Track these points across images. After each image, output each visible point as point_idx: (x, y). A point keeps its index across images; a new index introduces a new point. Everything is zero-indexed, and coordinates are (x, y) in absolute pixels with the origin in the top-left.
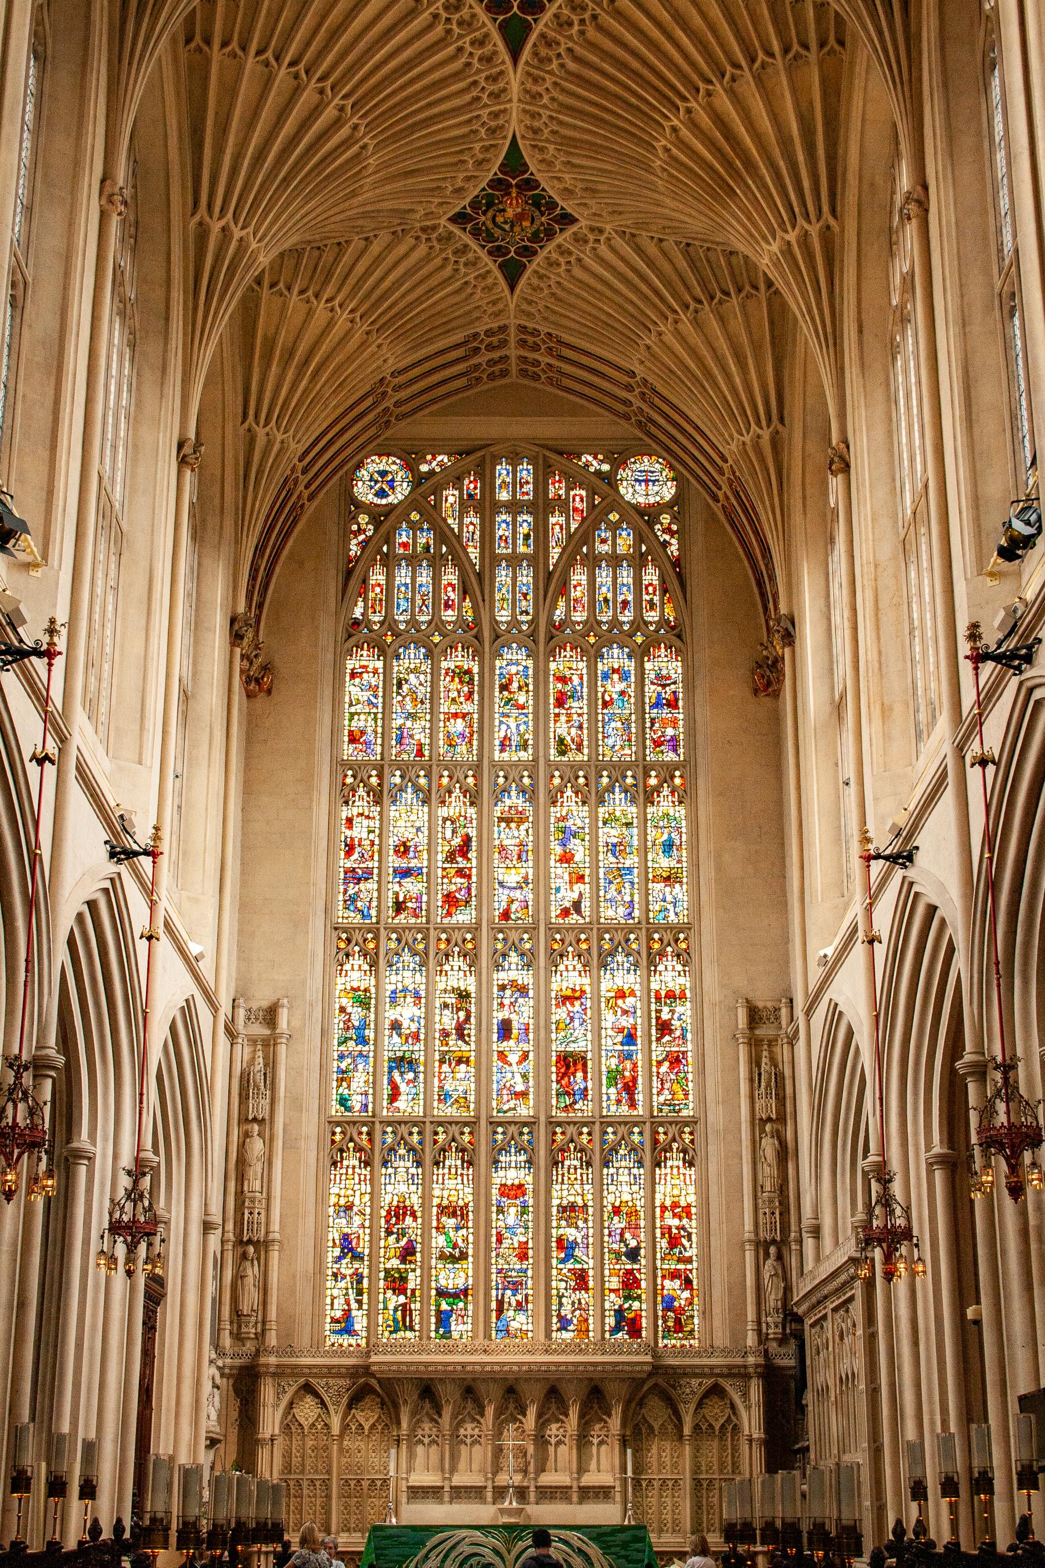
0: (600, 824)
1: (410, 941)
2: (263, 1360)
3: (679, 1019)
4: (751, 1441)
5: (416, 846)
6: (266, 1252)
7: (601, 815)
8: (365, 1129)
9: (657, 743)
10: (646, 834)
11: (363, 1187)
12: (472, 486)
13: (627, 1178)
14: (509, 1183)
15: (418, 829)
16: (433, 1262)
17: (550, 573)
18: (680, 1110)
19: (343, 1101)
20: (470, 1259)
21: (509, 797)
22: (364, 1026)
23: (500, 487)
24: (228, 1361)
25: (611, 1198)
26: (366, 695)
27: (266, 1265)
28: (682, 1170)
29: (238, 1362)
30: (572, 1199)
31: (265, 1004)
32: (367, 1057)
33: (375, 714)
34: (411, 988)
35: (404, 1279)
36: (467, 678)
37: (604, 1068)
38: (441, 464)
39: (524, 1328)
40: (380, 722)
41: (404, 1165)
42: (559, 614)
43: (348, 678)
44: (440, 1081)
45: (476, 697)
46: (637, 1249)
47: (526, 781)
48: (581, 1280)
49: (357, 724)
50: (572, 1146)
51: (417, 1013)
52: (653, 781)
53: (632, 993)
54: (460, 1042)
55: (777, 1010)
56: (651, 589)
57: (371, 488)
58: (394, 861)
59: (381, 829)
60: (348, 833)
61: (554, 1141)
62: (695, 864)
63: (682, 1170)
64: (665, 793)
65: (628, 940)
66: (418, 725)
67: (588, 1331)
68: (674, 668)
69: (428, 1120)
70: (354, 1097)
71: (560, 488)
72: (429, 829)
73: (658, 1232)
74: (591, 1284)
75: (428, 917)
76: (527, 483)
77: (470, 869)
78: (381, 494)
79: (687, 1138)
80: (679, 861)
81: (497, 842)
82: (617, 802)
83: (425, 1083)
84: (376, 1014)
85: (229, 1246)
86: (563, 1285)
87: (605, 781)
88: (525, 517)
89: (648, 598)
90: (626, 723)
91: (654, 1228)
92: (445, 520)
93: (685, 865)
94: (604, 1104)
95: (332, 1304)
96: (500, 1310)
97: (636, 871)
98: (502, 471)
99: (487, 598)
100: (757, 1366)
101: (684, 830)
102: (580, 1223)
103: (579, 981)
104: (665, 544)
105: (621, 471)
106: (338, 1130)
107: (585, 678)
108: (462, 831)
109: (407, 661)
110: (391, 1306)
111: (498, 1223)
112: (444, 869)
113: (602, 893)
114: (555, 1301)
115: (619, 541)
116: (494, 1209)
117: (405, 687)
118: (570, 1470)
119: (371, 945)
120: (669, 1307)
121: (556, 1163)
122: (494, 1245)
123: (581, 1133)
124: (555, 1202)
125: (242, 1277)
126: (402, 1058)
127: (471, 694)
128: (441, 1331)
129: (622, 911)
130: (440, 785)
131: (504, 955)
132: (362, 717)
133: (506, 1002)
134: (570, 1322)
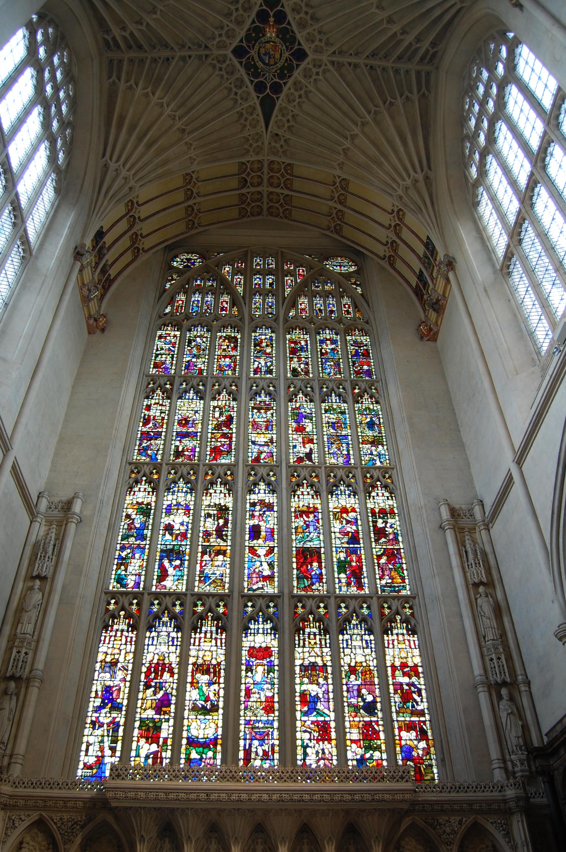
3: (391, 527)
5: (194, 420)
6: (27, 688)
11: (129, 647)
13: (360, 643)
14: (257, 646)
15: (196, 412)
16: (186, 713)
18: (399, 591)
19: (120, 580)
20: (221, 711)
21: (260, 396)
22: (144, 526)
23: (256, 265)
25: (347, 659)
26: (167, 346)
30: (312, 660)
31: (65, 499)
32: (144, 548)
34: (182, 503)
35: (158, 729)
36: (233, 340)
37: (335, 560)
44: (201, 567)
45: (239, 348)
46: (374, 702)
50: (311, 617)
53: (354, 510)
54: (219, 540)
55: (471, 510)
56: (347, 306)
58: (177, 428)
61: (296, 613)
63: (406, 637)
68: (365, 339)
69: (189, 593)
73: (391, 687)
74: (333, 735)
80: (380, 433)
81: (251, 420)
82: (334, 401)
84: (154, 519)
86: (307, 736)
90: (337, 365)
91: (388, 685)
94: (337, 586)
97: (349, 437)
99: (247, 302)
102: (321, 681)
108: (227, 414)
110: (143, 753)
111: (247, 680)
112: (212, 433)
113: (326, 449)
114: (300, 751)
116: (244, 667)
117: (193, 344)
120: (408, 756)
124: (298, 662)
126: (172, 550)
129: (341, 460)
131: (256, 484)
132: (164, 356)
133: (257, 514)
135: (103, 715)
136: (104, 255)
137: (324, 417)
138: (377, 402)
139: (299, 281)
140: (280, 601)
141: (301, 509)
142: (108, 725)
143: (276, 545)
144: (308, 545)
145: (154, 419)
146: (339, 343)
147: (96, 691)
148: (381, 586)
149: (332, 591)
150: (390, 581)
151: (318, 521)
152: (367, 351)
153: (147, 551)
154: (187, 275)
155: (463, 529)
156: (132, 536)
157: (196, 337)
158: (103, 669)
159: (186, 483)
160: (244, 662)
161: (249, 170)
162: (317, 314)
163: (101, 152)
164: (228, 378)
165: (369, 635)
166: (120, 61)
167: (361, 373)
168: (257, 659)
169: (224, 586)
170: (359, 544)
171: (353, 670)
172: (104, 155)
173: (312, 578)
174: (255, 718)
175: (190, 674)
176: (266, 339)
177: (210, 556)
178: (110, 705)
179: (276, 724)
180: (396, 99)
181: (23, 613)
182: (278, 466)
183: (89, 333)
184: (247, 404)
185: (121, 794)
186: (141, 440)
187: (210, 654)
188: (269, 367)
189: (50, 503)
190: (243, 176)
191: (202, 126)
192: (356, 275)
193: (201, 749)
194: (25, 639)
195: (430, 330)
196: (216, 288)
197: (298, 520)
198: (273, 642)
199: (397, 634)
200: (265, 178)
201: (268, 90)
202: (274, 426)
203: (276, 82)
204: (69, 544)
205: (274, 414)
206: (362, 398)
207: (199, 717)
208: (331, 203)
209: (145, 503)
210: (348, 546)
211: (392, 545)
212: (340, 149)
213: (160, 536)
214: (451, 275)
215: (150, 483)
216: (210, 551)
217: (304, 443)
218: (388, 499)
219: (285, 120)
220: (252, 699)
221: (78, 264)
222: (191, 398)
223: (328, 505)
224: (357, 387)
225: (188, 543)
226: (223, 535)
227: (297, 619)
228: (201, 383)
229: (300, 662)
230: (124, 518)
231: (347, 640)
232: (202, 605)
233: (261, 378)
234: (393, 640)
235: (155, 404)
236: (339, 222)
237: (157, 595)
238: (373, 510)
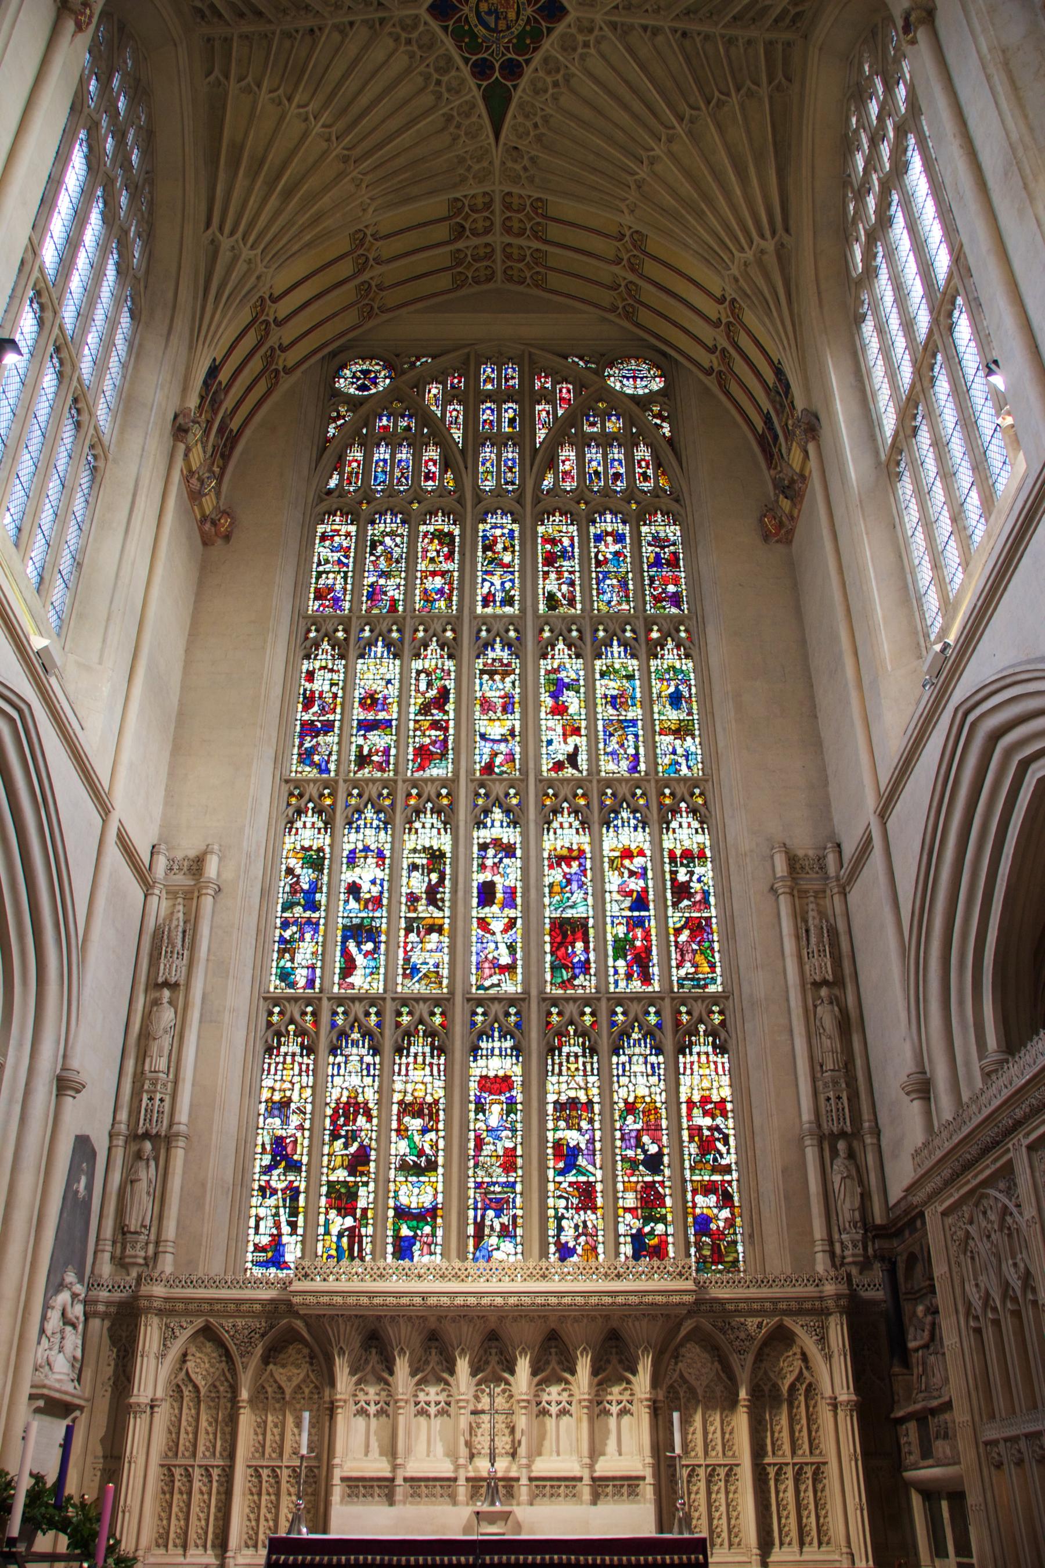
2: (144, 1290)
3: (699, 881)
4: (835, 1407)
5: (385, 698)
6: (168, 1150)
7: (597, 668)
9: (658, 599)
10: (650, 687)
11: (304, 1078)
13: (642, 1068)
14: (491, 1074)
15: (389, 682)
18: (706, 986)
19: (285, 976)
20: (440, 1170)
21: (493, 649)
22: (315, 888)
23: (485, 381)
24: (104, 1294)
25: (623, 1093)
26: (336, 556)
28: (712, 1058)
29: (117, 1296)
30: (572, 1094)
31: (192, 853)
32: (317, 924)
33: (346, 573)
34: (373, 847)
35: (354, 1196)
37: (609, 937)
41: (357, 1053)
42: (548, 482)
44: (406, 952)
45: (456, 556)
46: (660, 1155)
48: (586, 1195)
50: (571, 1029)
51: (380, 875)
52: (655, 635)
53: (641, 853)
54: (431, 908)
55: (821, 859)
56: (643, 464)
58: (359, 713)
61: (548, 1023)
62: (708, 712)
63: (712, 1058)
65: (634, 795)
68: (673, 532)
69: (389, 996)
70: (298, 971)
72: (401, 681)
74: (599, 1202)
76: (513, 378)
77: (447, 721)
78: (363, 388)
80: (690, 714)
81: (479, 694)
82: (616, 655)
83: (387, 954)
84: (329, 874)
85: (120, 1141)
86: (562, 1203)
90: (624, 584)
91: (681, 1129)
94: (611, 980)
95: (257, 1227)
96: (479, 1236)
97: (640, 723)
98: (488, 371)
99: (470, 465)
100: (838, 1297)
101: (693, 682)
102: (584, 1125)
103: (576, 839)
107: (576, 539)
108: (438, 684)
110: (335, 1230)
112: (416, 721)
113: (601, 746)
114: (552, 1224)
116: (472, 1107)
117: (380, 549)
118: (579, 1453)
122: (472, 1153)
123: (583, 1014)
124: (551, 1098)
126: (360, 926)
129: (625, 764)
131: (487, 812)
132: (331, 576)
133: (489, 862)
135: (275, 1177)
136: (221, 403)
138: (687, 656)
139: (560, 412)
140: (525, 1005)
141: (559, 852)
142: (284, 1191)
144: (569, 913)
145: (320, 697)
146: (628, 541)
147: (263, 1145)
149: (603, 989)
150: (692, 970)
151: (584, 872)
152: (675, 554)
153: (322, 928)
154: (363, 410)
155: (806, 891)
156: (299, 904)
157: (384, 534)
159: (377, 812)
160: (472, 1098)
161: (467, 209)
162: (591, 481)
163: (203, 217)
164: (439, 617)
165: (657, 1055)
166: (226, 39)
167: (664, 600)
168: (491, 1094)
169: (441, 983)
170: (648, 910)
171: (630, 1108)
172: (208, 225)
173: (573, 968)
175: (395, 1118)
176: (503, 535)
177: (418, 934)
178: (283, 1164)
180: (728, 95)
181: (151, 1042)
182: (522, 780)
183: (205, 544)
184: (471, 666)
185: (312, 1300)
186: (302, 737)
187: (423, 1087)
188: (507, 592)
189: (171, 860)
190: (458, 220)
191: (379, 146)
192: (660, 399)
193: (415, 1223)
194: (157, 1079)
195: (781, 525)
196: (415, 435)
197: (552, 871)
198: (515, 1068)
199: (699, 1054)
200: (498, 221)
201: (497, 74)
203: (510, 60)
204: (205, 930)
205: (517, 683)
206: (662, 649)
208: (616, 269)
210: (629, 914)
211: (699, 911)
212: (630, 179)
214: (811, 447)
215: (320, 813)
216: (418, 928)
217: (565, 735)
219: (529, 124)
220: (484, 1153)
221: (182, 447)
223: (601, 846)
224: (655, 628)
225: (385, 914)
226: (436, 900)
227: (550, 1034)
228: (394, 628)
229: (554, 1097)
231: (623, 1064)
232: (409, 1013)
233: (495, 616)
234: (692, 1063)
235: (322, 668)
236: (630, 301)
237: (340, 1001)
238: (672, 853)
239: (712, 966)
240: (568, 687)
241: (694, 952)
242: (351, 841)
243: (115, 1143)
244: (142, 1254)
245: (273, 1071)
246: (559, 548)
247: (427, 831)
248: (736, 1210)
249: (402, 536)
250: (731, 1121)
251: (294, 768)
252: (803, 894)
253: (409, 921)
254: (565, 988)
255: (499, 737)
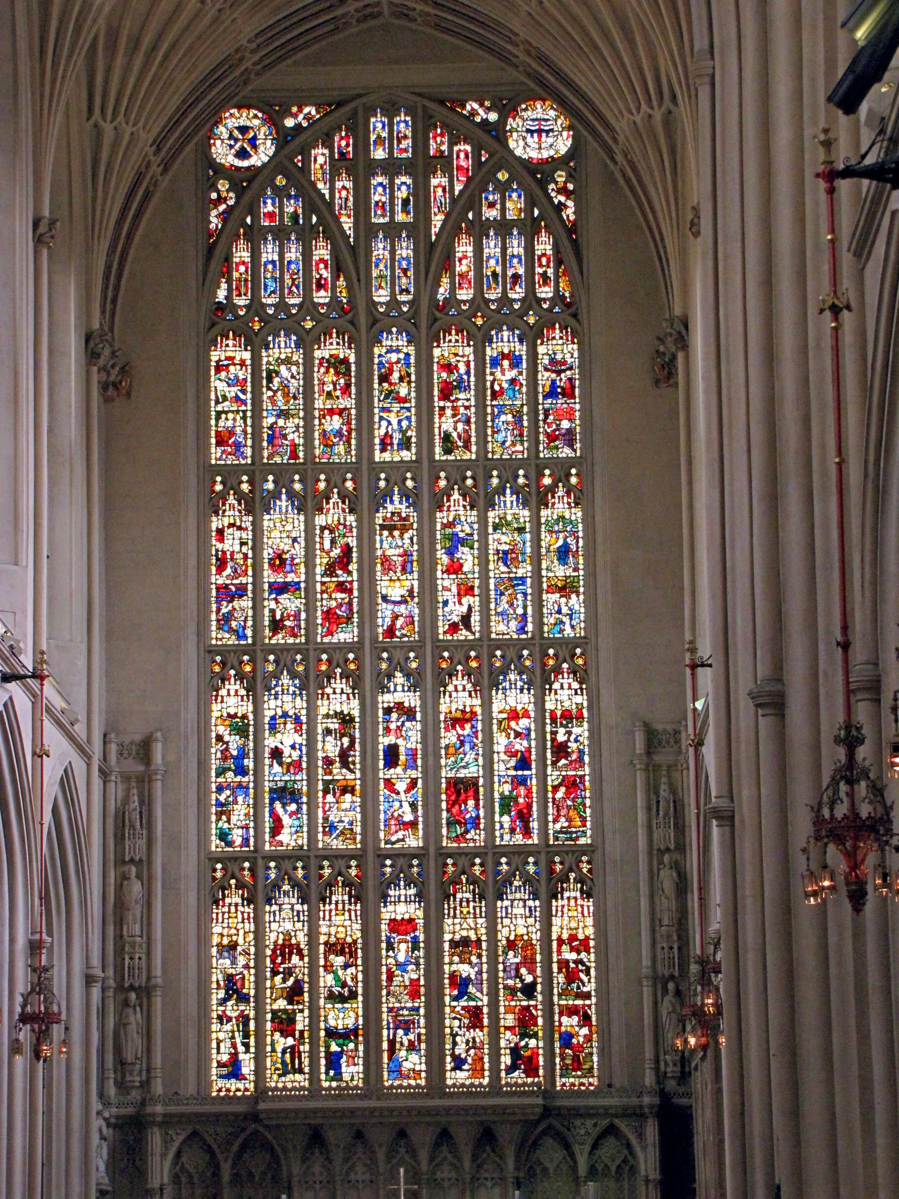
0: (490, 530)
1: (289, 663)
2: (149, 1109)
3: (576, 741)
4: (647, 1181)
5: (293, 559)
6: (149, 998)
7: (490, 520)
8: (247, 865)
9: (552, 437)
11: (247, 925)
12: (343, 143)
13: (521, 911)
14: (399, 917)
15: (295, 540)
16: (322, 1002)
17: (432, 246)
18: (577, 838)
19: (223, 836)
20: (360, 998)
21: (392, 502)
22: (243, 754)
24: (114, 1110)
25: (505, 932)
26: (233, 391)
27: (149, 1012)
28: (580, 902)
29: (123, 1111)
30: (464, 933)
31: (138, 738)
32: (247, 788)
33: (244, 412)
34: (291, 713)
35: (292, 1021)
37: (497, 795)
38: (307, 117)
39: (417, 1068)
40: (249, 421)
41: (289, 901)
42: (443, 292)
43: (213, 372)
44: (324, 812)
46: (533, 984)
47: (410, 484)
48: (475, 1017)
49: (225, 423)
50: (464, 878)
52: (547, 481)
53: (526, 714)
54: (344, 770)
56: (544, 260)
57: (231, 147)
58: (269, 576)
59: (254, 540)
60: (219, 546)
61: (445, 873)
63: (580, 902)
64: (560, 494)
66: (291, 423)
67: (483, 1070)
68: (569, 352)
71: (442, 143)
72: (306, 540)
73: (555, 967)
74: (486, 1021)
75: (307, 635)
76: (405, 137)
77: (351, 582)
78: (242, 154)
79: (585, 868)
80: (576, 569)
82: (509, 505)
83: (309, 814)
84: (255, 742)
86: (457, 1023)
87: (495, 481)
88: (404, 179)
89: (540, 270)
90: (518, 417)
91: (551, 962)
92: (314, 184)
93: (581, 572)
94: (497, 833)
96: (392, 1050)
97: (529, 581)
98: (377, 125)
99: (362, 277)
100: (651, 1106)
101: (581, 534)
102: (474, 959)
103: (469, 702)
104: (561, 206)
105: (510, 120)
106: (219, 866)
107: (472, 365)
108: (341, 541)
109: (277, 351)
110: (279, 1048)
112: (323, 583)
113: (492, 606)
114: (448, 1040)
115: (509, 205)
116: (384, 945)
117: (276, 380)
119: (248, 668)
121: (448, 897)
122: (385, 984)
124: (447, 937)
125: (125, 1025)
126: (284, 789)
127: (348, 386)
128: (332, 1073)
129: (513, 625)
130: (317, 490)
131: (390, 676)
133: (393, 726)
134: (464, 1061)
135: (229, 1008)
137: (491, 542)
140: (425, 860)
141: (454, 714)
142: (237, 1018)
143: (420, 775)
144: (462, 774)
145: (232, 559)
146: (524, 365)
147: (218, 982)
148: (555, 832)
151: (476, 733)
153: (252, 791)
155: (659, 766)
156: (229, 769)
157: (280, 362)
158: (220, 953)
160: (384, 938)
165: (534, 900)
168: (399, 934)
169: (355, 839)
170: (530, 769)
171: (511, 945)
173: (465, 824)
174: (397, 1005)
175: (322, 956)
176: (398, 362)
179: (422, 1011)
184: (372, 519)
186: (218, 602)
187: (343, 930)
193: (341, 1041)
199: (569, 898)
202: (415, 564)
204: (158, 812)
205: (415, 539)
207: (336, 1006)
209: (239, 715)
211: (575, 769)
213: (267, 768)
216: (334, 789)
217: (460, 596)
218: (576, 694)
220: (395, 983)
222: (284, 510)
225: (305, 777)
229: (451, 936)
230: (214, 740)
231: (506, 908)
234: (563, 906)
235: (231, 525)
237: (271, 857)
238: (553, 713)
239: (584, 821)
240: (463, 542)
241: (569, 807)
242: (271, 707)
243: (107, 994)
244: (138, 1079)
245: (220, 920)
246: (454, 377)
247: (338, 696)
248: (594, 1028)
249: (297, 364)
250: (592, 955)
251: (214, 635)
252: (657, 768)
253: (326, 783)
254: (459, 842)
255: (399, 599)
